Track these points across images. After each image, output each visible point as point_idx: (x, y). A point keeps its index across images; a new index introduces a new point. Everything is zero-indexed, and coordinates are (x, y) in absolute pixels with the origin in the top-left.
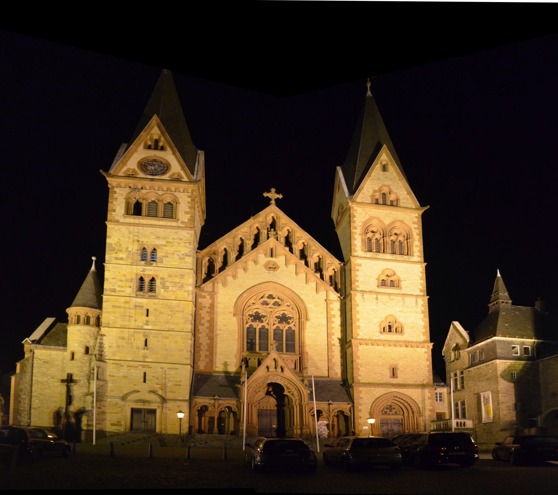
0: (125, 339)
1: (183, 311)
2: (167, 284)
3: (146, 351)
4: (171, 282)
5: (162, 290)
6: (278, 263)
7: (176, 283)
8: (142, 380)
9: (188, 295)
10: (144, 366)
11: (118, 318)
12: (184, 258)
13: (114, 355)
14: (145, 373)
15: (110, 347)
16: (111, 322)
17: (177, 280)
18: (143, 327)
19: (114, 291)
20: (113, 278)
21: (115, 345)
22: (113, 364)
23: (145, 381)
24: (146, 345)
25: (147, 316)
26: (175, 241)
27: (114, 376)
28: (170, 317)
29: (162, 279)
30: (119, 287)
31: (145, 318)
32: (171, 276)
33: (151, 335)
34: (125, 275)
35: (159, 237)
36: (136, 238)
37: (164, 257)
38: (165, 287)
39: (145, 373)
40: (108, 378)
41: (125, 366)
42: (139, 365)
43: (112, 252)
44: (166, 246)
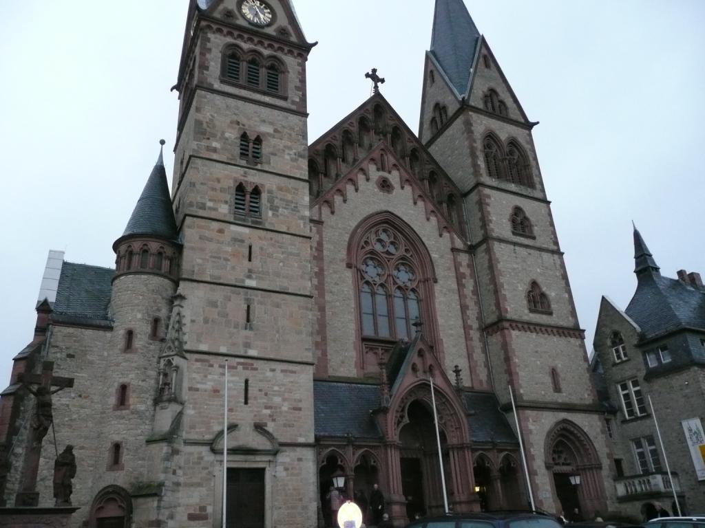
0: (217, 307)
1: (298, 255)
2: (277, 202)
3: (248, 333)
4: (281, 199)
5: (270, 213)
6: (391, 180)
7: (287, 201)
8: (243, 401)
9: (305, 223)
10: (245, 366)
11: (208, 260)
12: (296, 160)
13: (199, 341)
14: (246, 382)
15: (193, 321)
16: (196, 269)
17: (289, 197)
18: (243, 281)
19: (203, 207)
20: (202, 184)
21: (202, 319)
22: (197, 360)
23: (246, 403)
24: (248, 320)
25: (250, 260)
26: (286, 130)
27: (197, 390)
28: (281, 264)
29: (270, 192)
30: (210, 200)
31: (246, 261)
32: (280, 189)
33: (256, 299)
34: (218, 180)
35: (264, 121)
36: (235, 118)
37: (272, 154)
38: (274, 209)
39: (246, 382)
40: (185, 395)
41: (216, 366)
42: (239, 363)
43: (202, 137)
44: (274, 137)
